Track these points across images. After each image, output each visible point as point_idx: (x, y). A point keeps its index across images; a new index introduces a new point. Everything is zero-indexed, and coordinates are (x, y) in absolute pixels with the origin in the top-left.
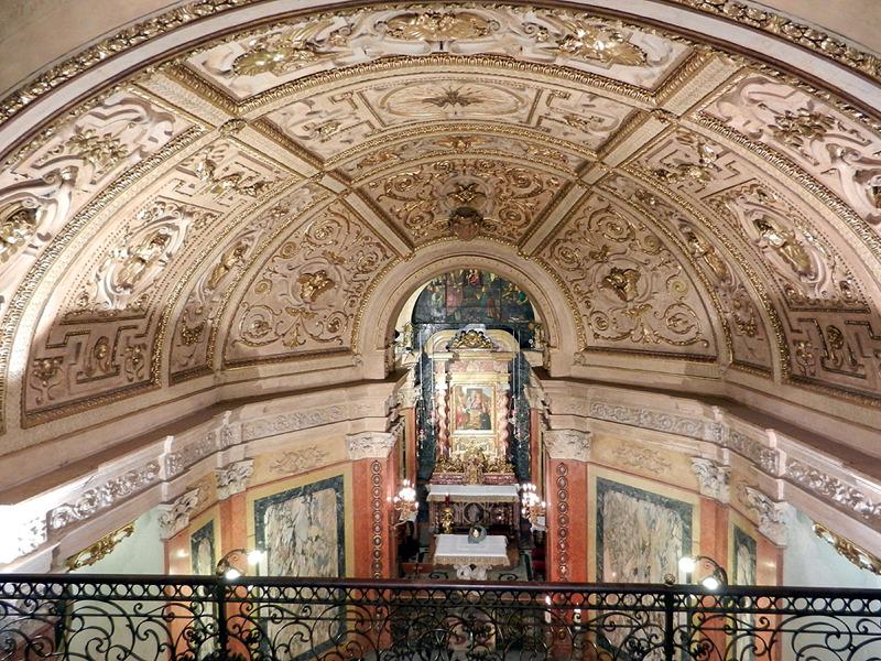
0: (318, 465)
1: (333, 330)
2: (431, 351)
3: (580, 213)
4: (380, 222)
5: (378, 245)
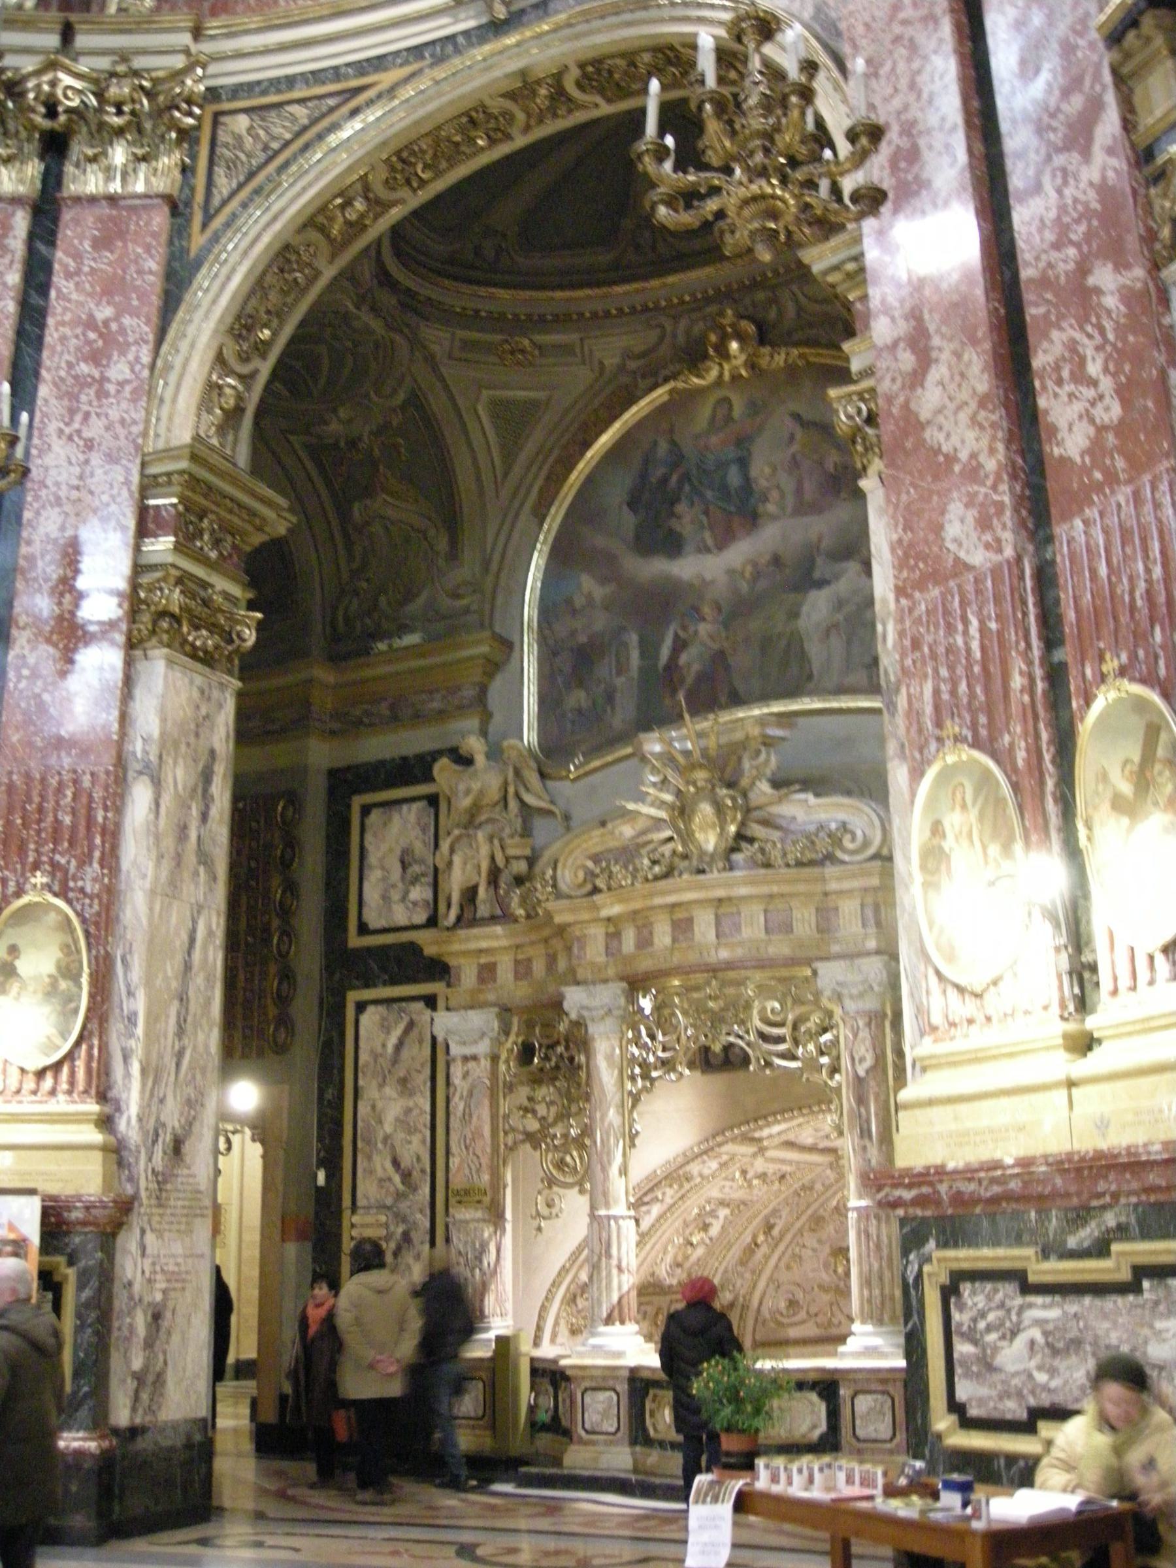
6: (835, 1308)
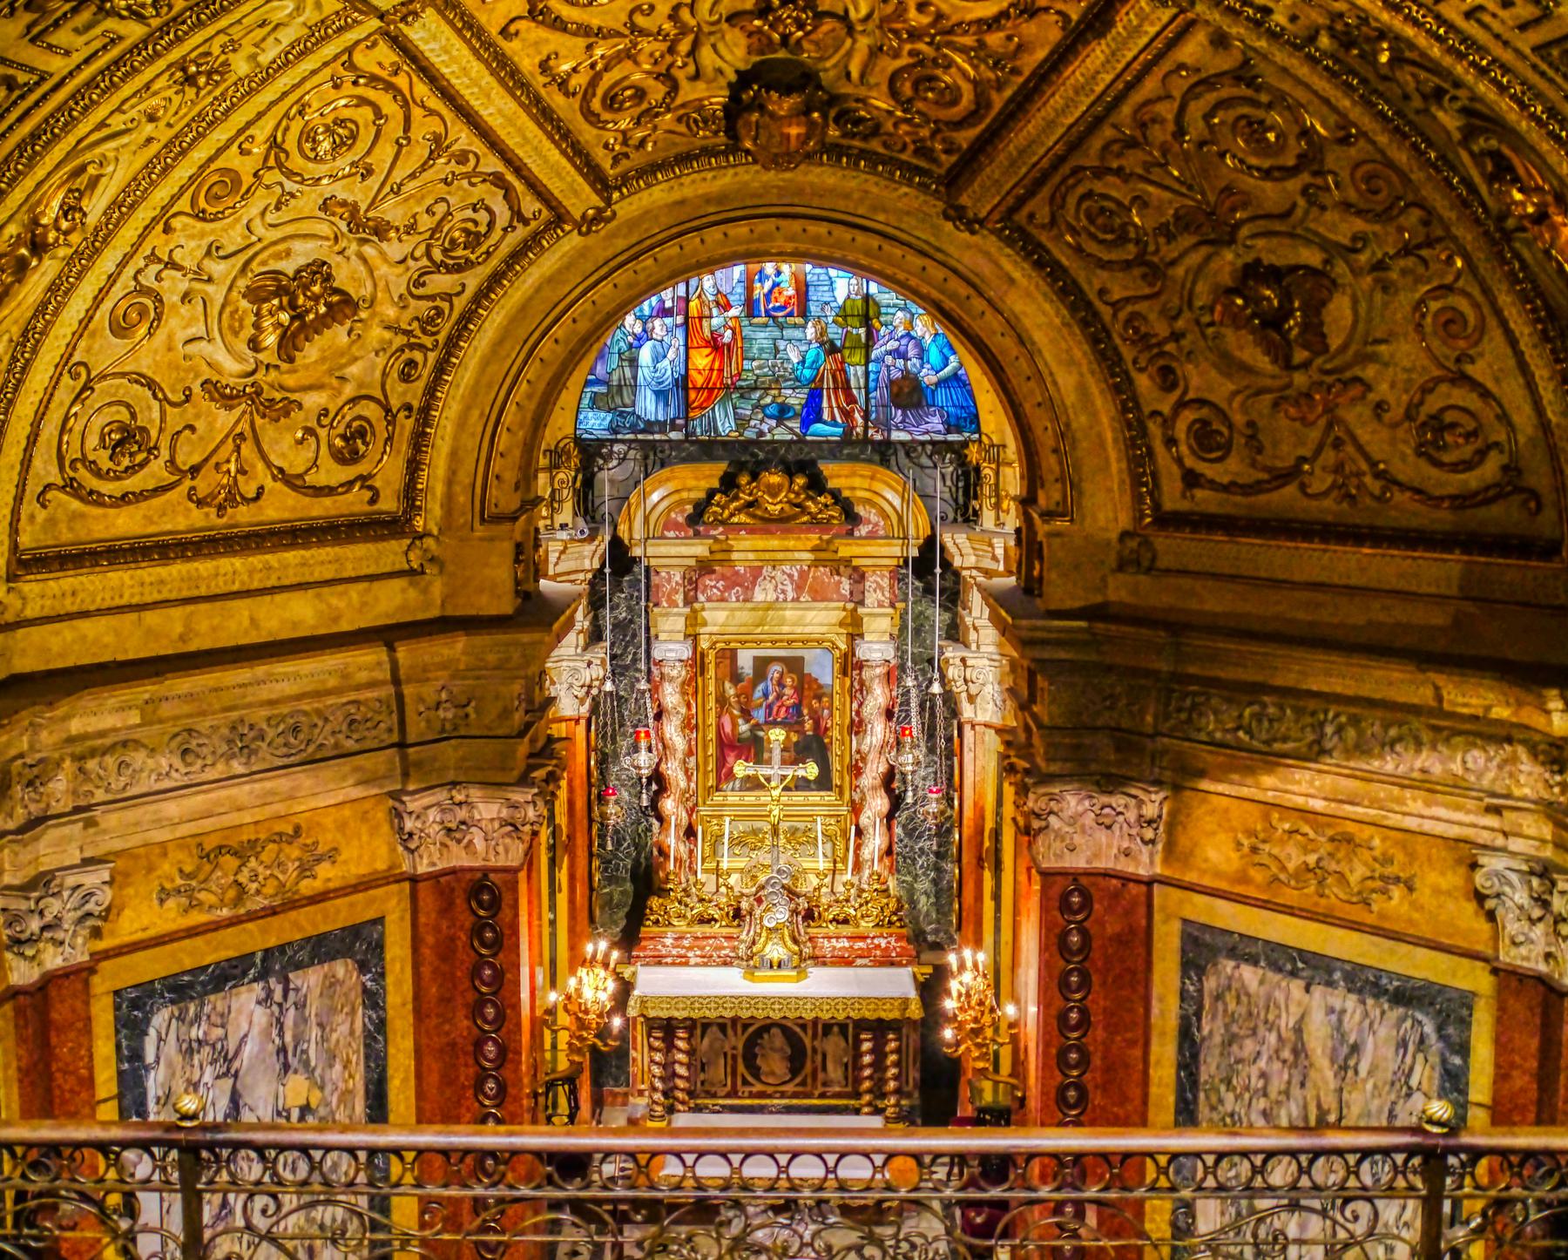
0: (307, 887)
1: (350, 456)
2: (638, 534)
3: (1150, 86)
4: (511, 106)
5: (498, 180)
6: (247, 449)
